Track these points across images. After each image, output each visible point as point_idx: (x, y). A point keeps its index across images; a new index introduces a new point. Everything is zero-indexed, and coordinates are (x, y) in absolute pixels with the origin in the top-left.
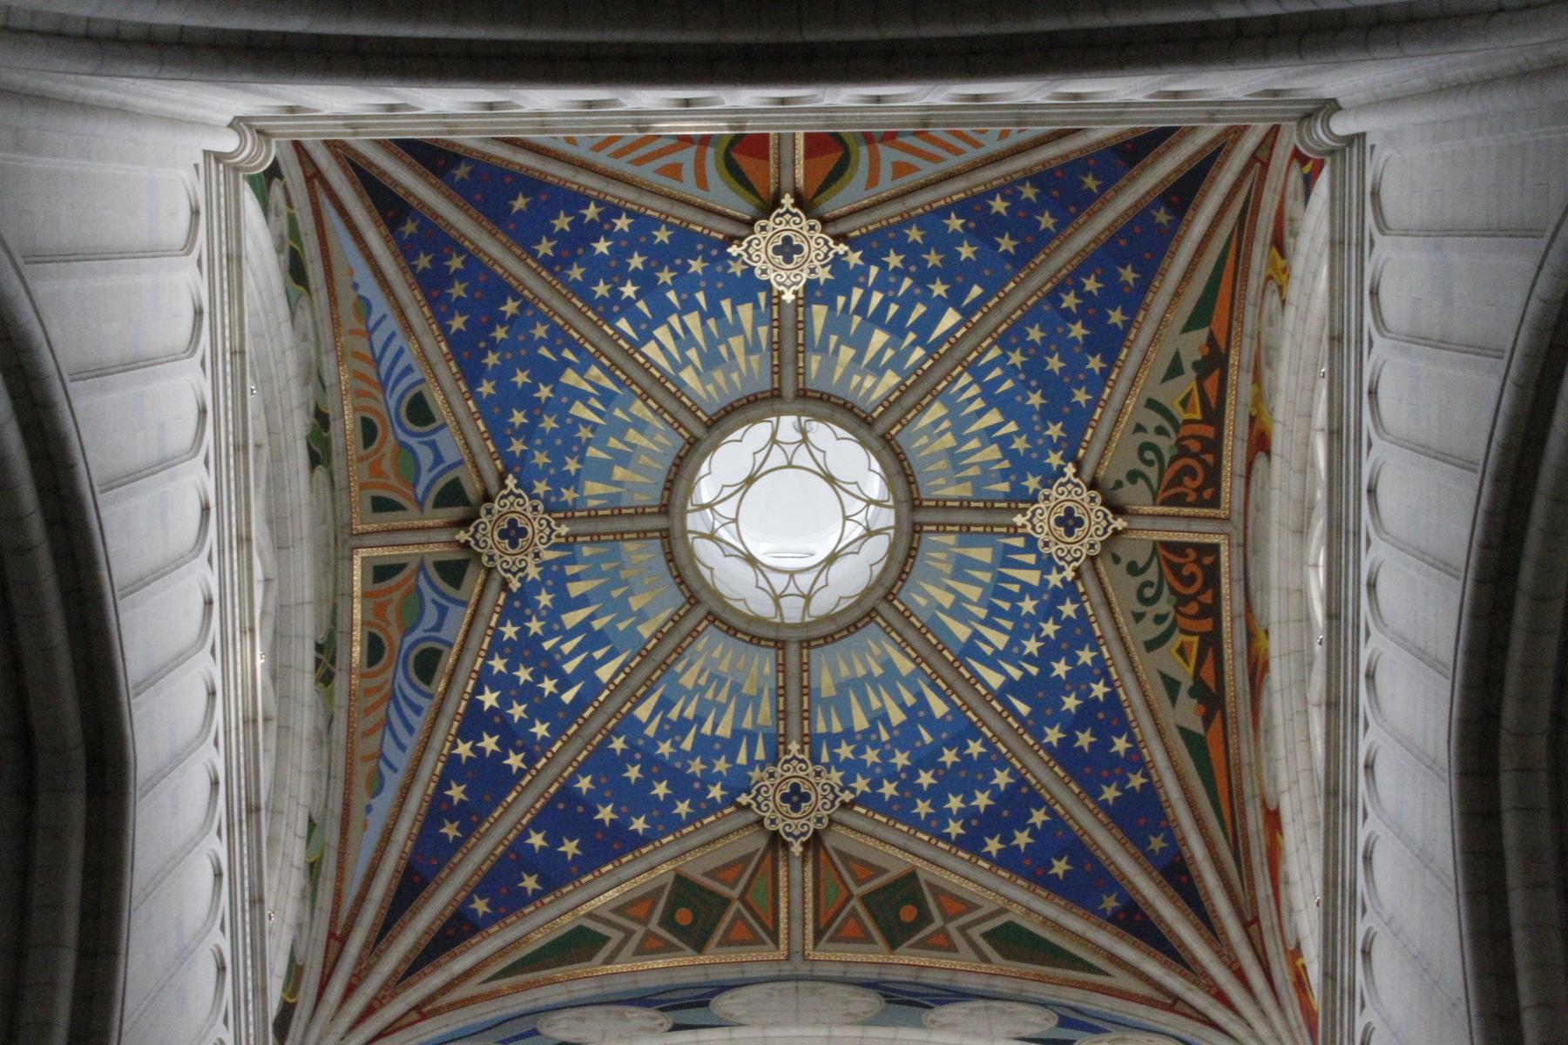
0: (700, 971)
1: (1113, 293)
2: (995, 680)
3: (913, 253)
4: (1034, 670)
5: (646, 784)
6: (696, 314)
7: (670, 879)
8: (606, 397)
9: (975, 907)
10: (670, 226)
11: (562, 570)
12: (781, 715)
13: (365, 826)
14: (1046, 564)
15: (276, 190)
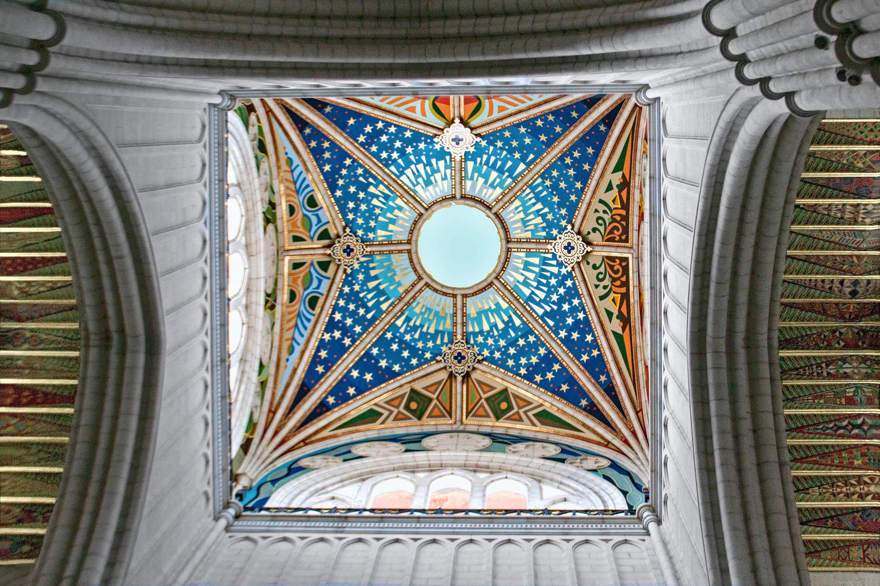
0: (420, 428)
1: (585, 158)
2: (540, 311)
3: (506, 141)
4: (555, 307)
5: (399, 351)
6: (422, 165)
7: (408, 390)
8: (386, 197)
9: (530, 403)
10: (411, 130)
11: (368, 266)
12: (455, 324)
13: (286, 367)
14: (560, 265)
15: (253, 118)
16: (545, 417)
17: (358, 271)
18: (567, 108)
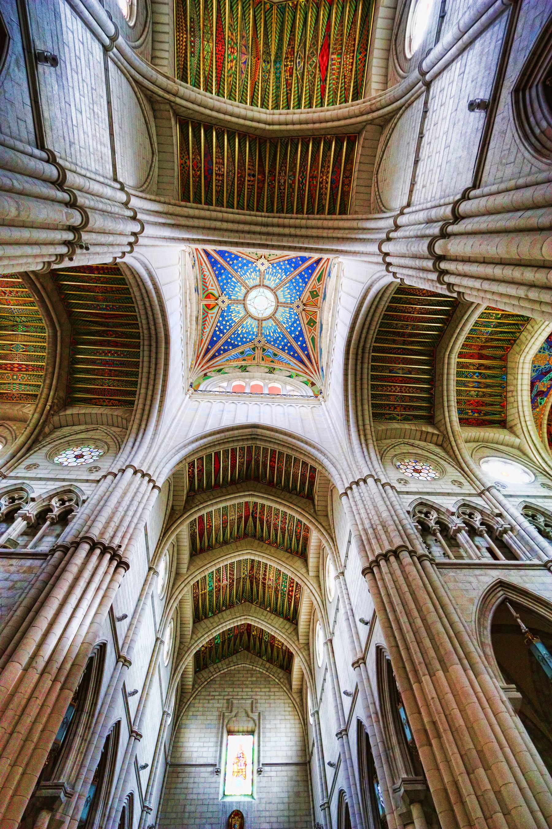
1: (230, 256)
2: (284, 276)
3: (224, 284)
5: (294, 327)
8: (243, 327)
12: (287, 307)
16: (319, 279)
18: (211, 262)
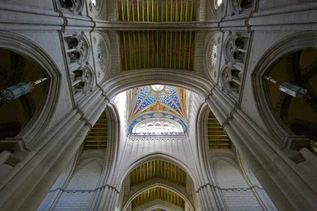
5: (149, 101)
16: (171, 111)
17: (142, 89)
